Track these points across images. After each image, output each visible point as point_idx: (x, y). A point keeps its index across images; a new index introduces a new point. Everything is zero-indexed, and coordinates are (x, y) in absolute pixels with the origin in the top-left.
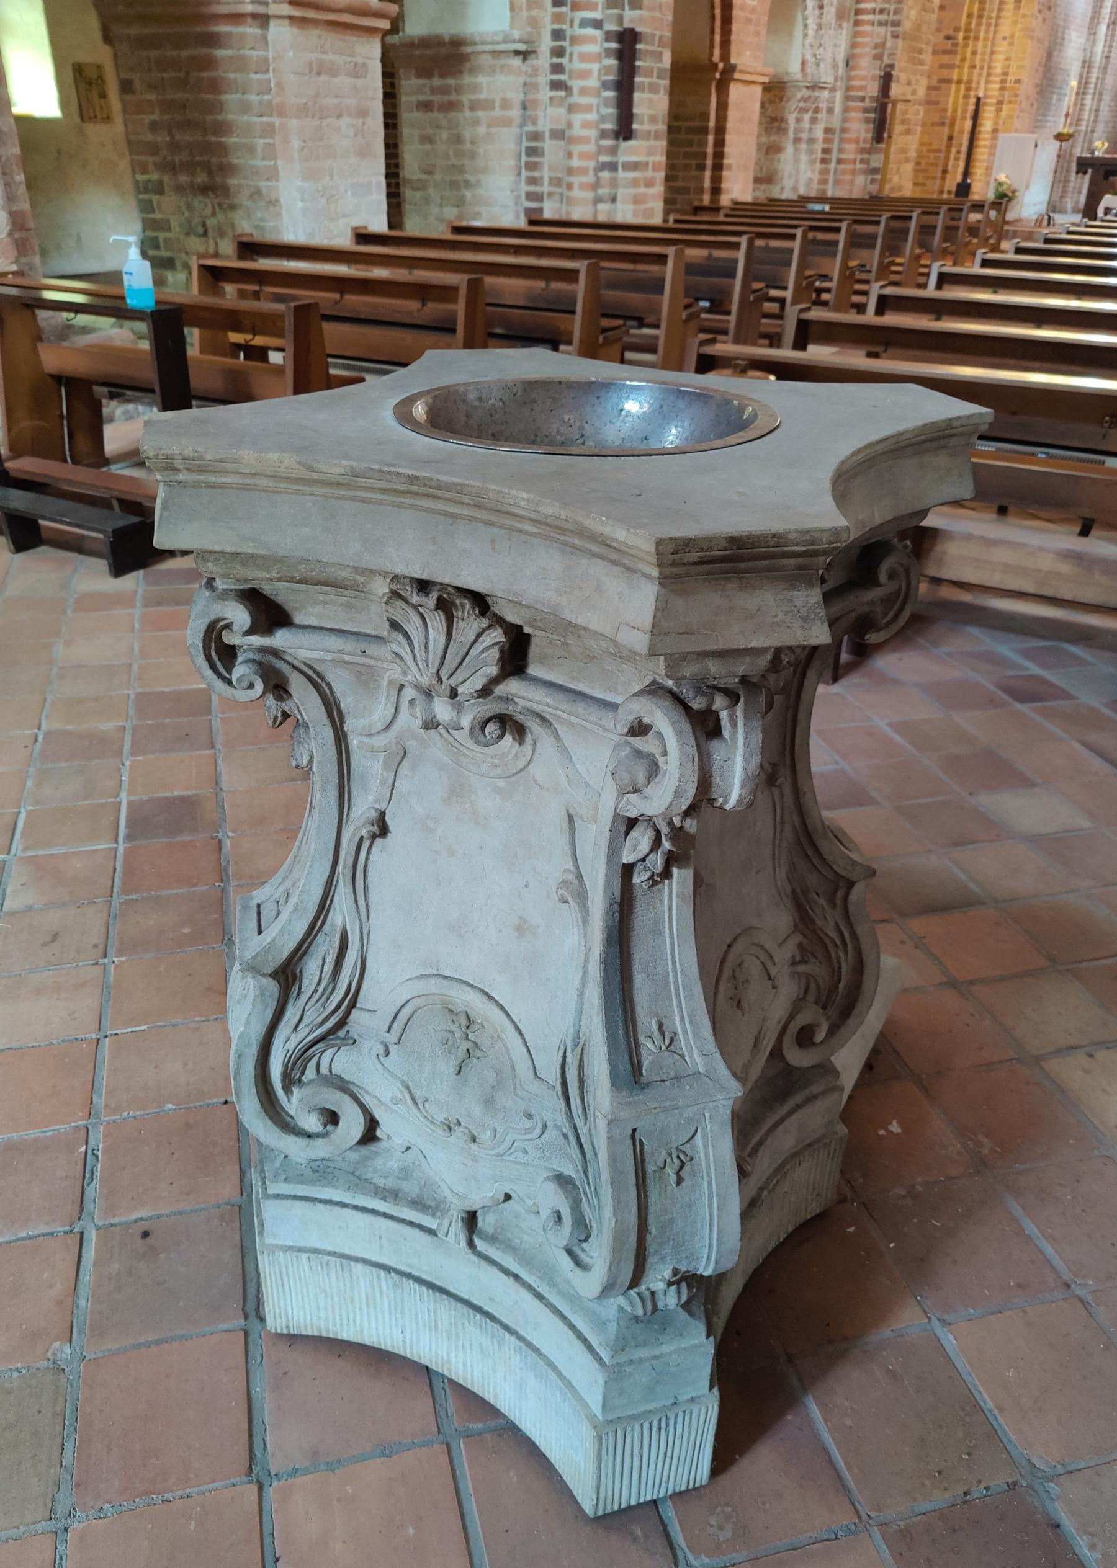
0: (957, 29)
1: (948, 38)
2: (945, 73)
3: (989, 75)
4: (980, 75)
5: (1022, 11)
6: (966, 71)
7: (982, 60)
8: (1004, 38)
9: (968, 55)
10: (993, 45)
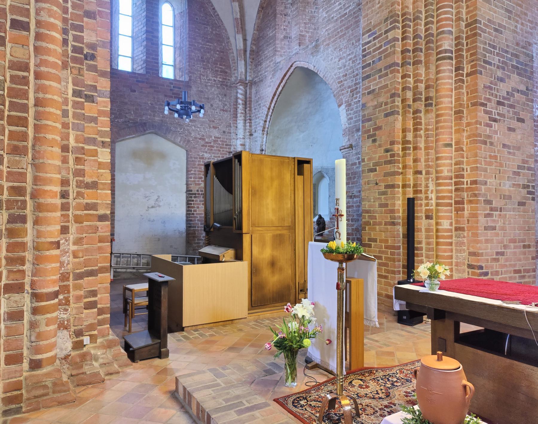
0: (392, 143)
1: (387, 151)
2: (390, 180)
3: (437, 178)
4: (427, 179)
5: (465, 121)
6: (410, 176)
7: (428, 166)
8: (450, 145)
9: (410, 163)
10: (437, 152)
